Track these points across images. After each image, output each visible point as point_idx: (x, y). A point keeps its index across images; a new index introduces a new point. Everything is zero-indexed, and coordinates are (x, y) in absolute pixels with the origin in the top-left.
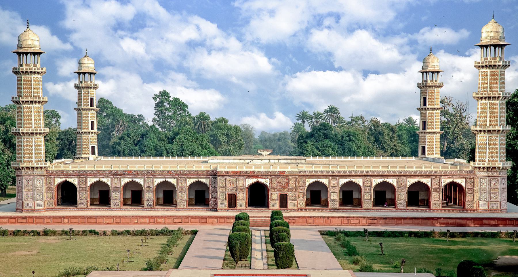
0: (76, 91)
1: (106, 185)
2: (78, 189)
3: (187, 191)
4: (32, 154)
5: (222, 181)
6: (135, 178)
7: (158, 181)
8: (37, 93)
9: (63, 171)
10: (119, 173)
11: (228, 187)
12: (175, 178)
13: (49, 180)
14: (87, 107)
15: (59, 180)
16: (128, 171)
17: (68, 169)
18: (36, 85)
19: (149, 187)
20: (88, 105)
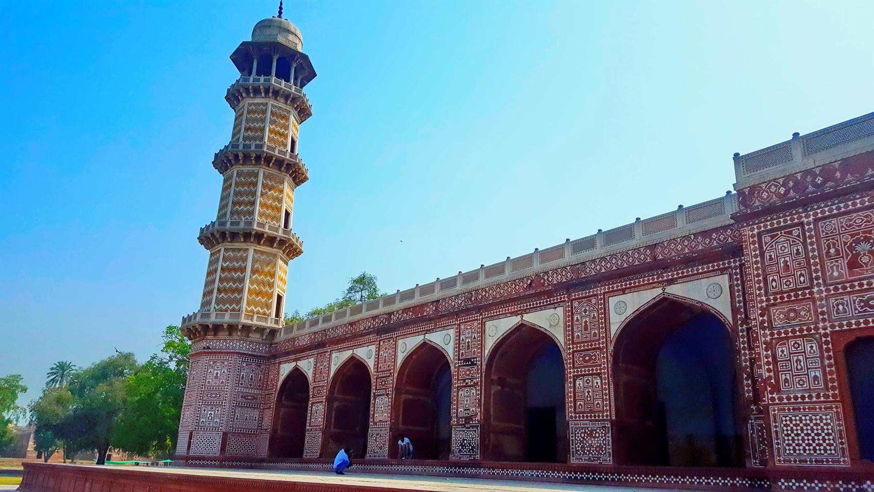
3: (604, 362)
5: (783, 250)
11: (839, 288)
19: (469, 362)
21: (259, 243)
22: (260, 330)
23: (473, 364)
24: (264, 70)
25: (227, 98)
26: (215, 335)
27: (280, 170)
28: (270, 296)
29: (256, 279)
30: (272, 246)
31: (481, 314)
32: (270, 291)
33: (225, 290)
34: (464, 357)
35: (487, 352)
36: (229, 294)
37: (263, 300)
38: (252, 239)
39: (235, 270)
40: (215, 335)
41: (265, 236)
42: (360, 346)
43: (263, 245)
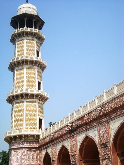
19: (105, 146)
21: (27, 98)
22: (33, 136)
23: (107, 146)
24: (22, 26)
25: (11, 41)
26: (15, 141)
27: (32, 65)
28: (35, 120)
29: (29, 114)
30: (33, 98)
32: (35, 118)
33: (17, 121)
36: (19, 122)
37: (33, 123)
38: (24, 97)
39: (20, 111)
40: (15, 141)
41: (29, 94)
42: (64, 140)
43: (30, 98)
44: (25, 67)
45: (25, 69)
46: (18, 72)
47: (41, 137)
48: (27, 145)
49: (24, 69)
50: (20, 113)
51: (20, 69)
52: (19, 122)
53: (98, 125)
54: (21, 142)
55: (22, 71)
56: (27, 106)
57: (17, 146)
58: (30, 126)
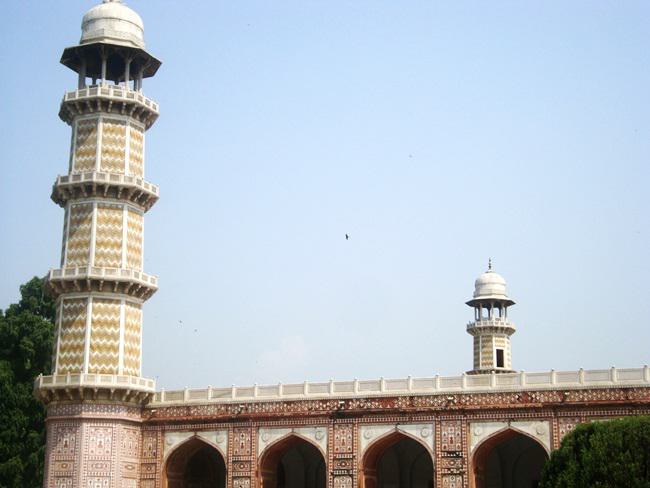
0: (471, 338)
1: (314, 450)
2: (230, 467)
4: (81, 348)
6: (404, 423)
7: (482, 432)
8: (113, 165)
9: (188, 408)
10: (353, 406)
12: (542, 419)
13: (150, 442)
14: (490, 367)
15: (176, 440)
16: (381, 399)
17: (201, 400)
18: (115, 141)
19: (453, 455)
20: (492, 364)
31: (466, 416)
34: (447, 449)
35: (472, 448)
36: (104, 353)
44: (127, 204)
45: (126, 212)
46: (105, 214)
47: (154, 403)
48: (123, 415)
49: (122, 209)
50: (110, 330)
51: (111, 208)
52: (104, 353)
53: (440, 422)
54: (113, 407)
55: (116, 215)
56: (127, 314)
57: (98, 415)
58: (100, 364)
